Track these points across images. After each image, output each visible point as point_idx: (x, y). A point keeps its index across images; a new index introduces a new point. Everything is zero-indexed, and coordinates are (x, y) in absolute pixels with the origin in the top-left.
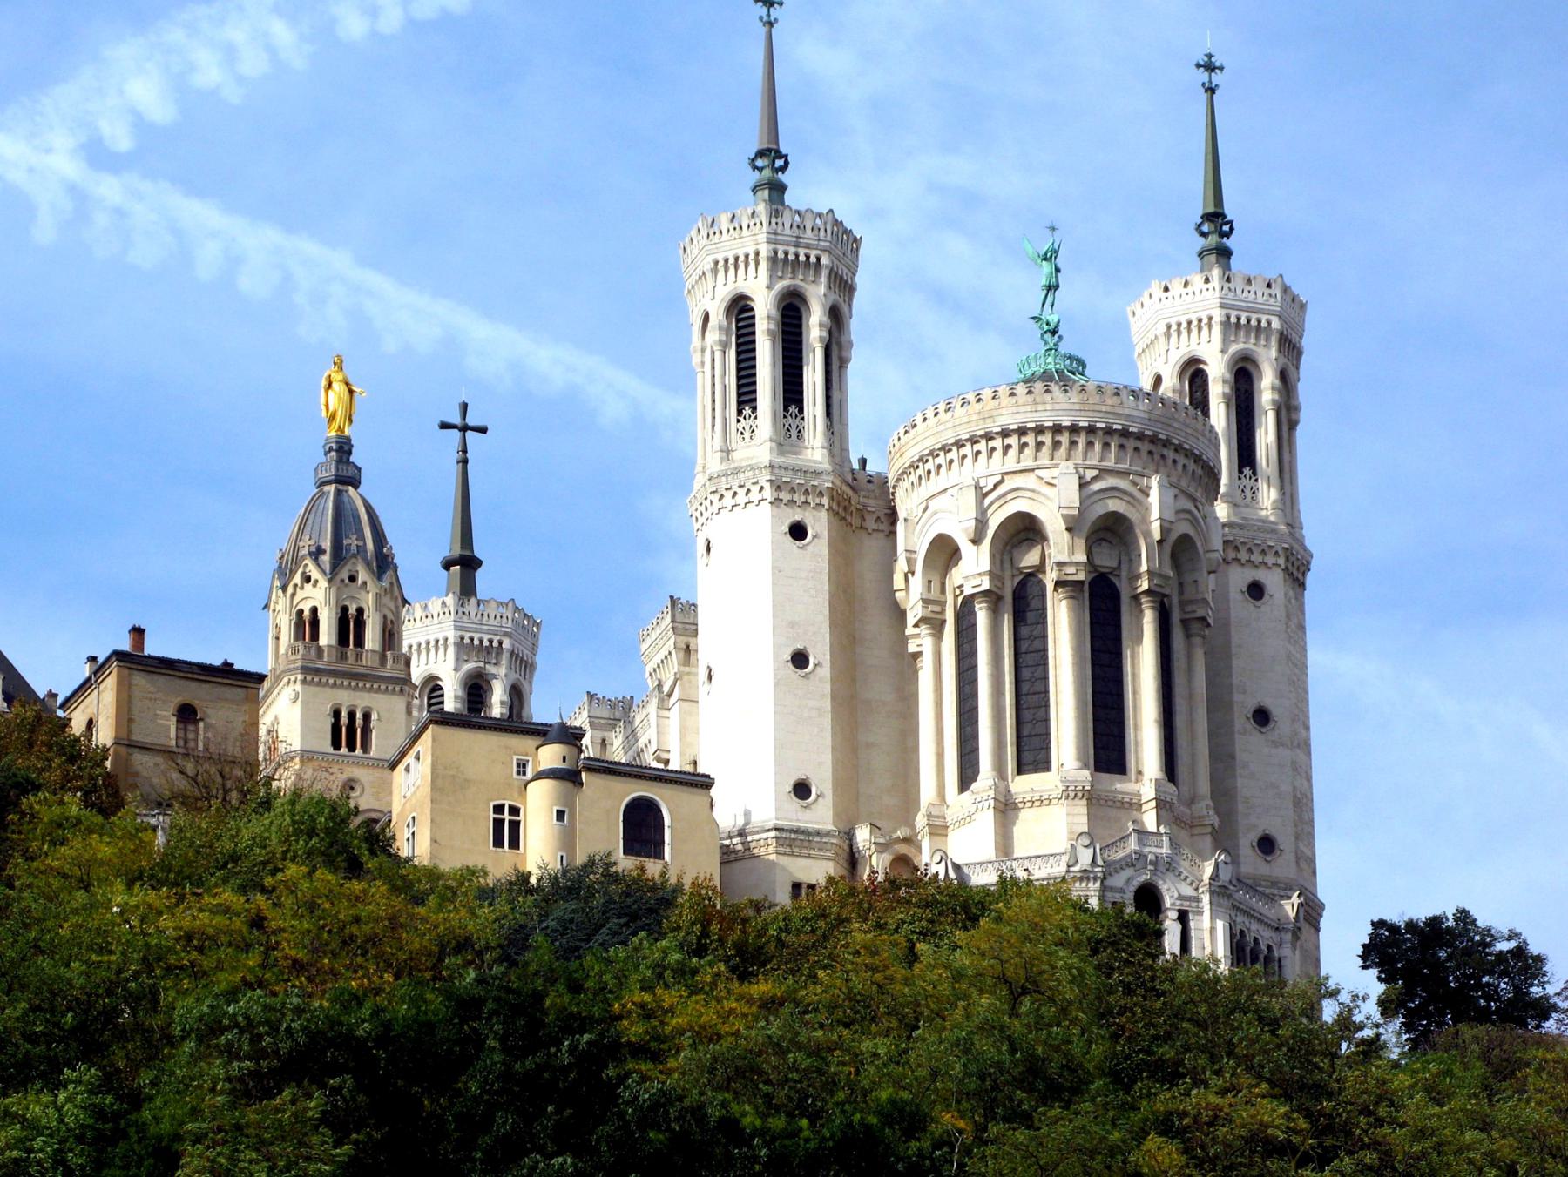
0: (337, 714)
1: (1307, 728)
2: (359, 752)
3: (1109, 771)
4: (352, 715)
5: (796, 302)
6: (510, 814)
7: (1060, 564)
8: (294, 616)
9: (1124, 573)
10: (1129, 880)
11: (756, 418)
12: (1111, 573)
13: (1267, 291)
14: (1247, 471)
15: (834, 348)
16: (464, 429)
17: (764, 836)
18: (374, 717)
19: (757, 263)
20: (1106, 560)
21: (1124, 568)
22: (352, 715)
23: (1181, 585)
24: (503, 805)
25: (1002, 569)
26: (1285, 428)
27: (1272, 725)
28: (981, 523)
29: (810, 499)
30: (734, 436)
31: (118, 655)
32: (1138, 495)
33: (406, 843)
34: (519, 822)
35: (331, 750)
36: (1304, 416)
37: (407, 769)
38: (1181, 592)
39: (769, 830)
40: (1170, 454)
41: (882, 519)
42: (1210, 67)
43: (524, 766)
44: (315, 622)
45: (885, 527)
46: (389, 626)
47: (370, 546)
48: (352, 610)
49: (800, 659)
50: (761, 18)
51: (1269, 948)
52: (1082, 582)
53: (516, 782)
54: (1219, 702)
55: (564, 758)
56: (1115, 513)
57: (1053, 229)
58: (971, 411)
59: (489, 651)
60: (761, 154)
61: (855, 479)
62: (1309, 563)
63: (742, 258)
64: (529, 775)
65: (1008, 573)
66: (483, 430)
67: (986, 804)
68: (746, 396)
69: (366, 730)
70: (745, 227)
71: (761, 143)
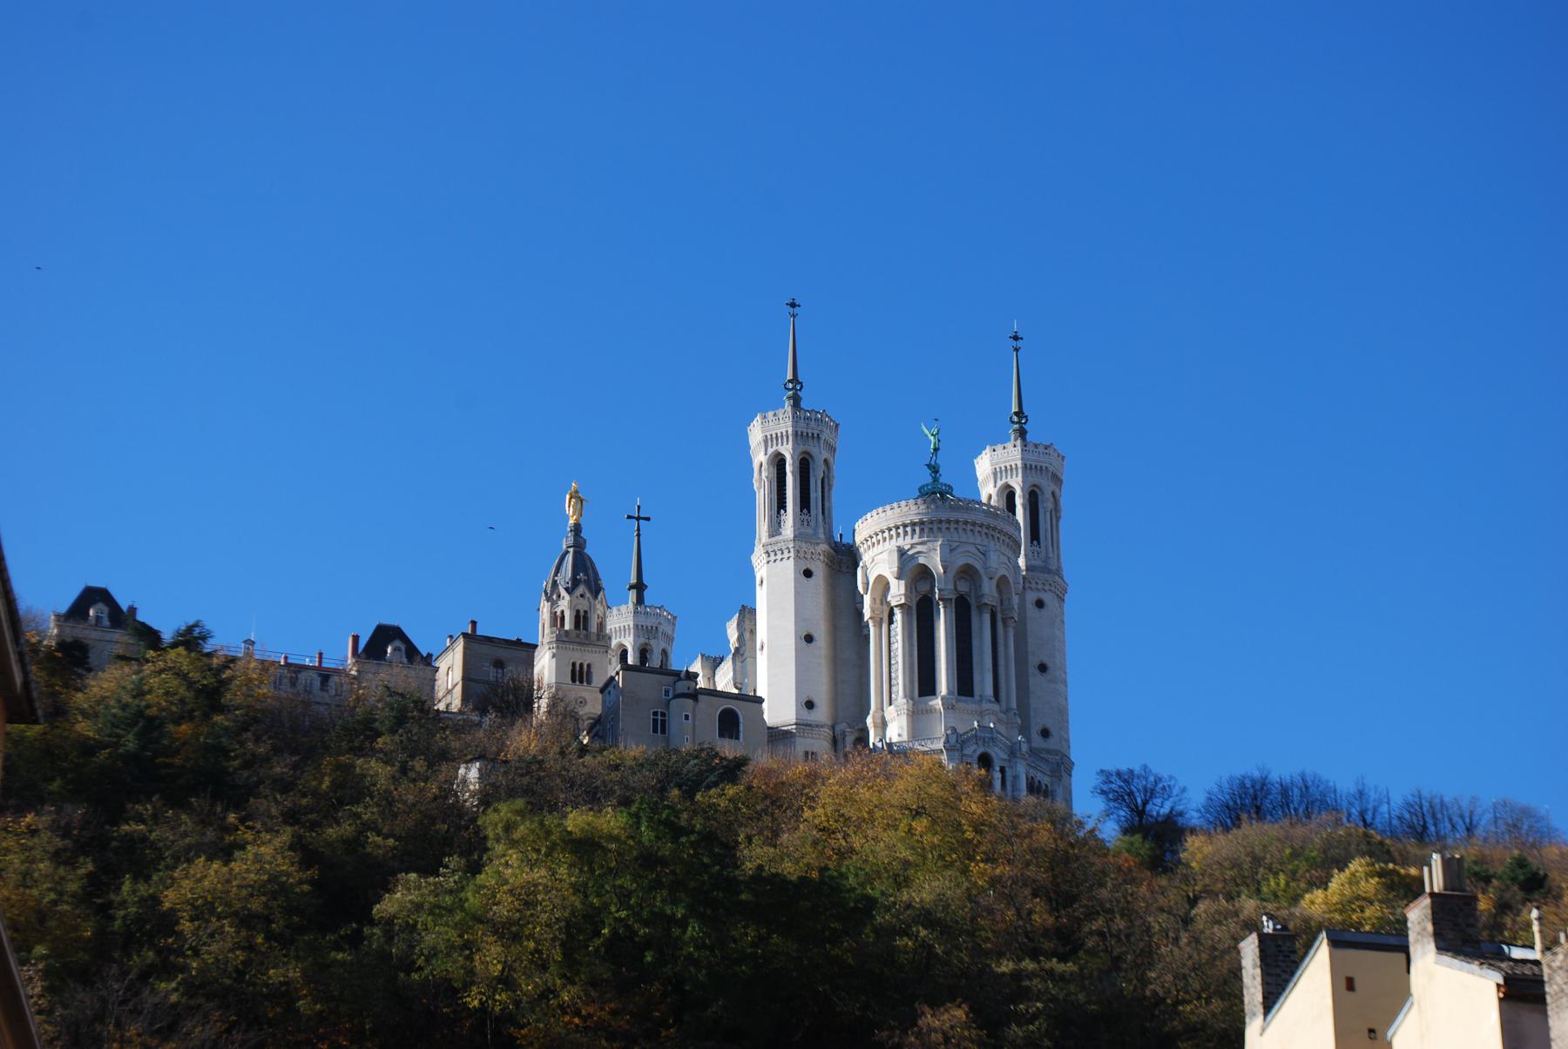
0: (574, 664)
2: (585, 684)
3: (965, 695)
4: (581, 665)
5: (807, 456)
9: (973, 595)
14: (1035, 542)
15: (826, 480)
16: (638, 519)
20: (963, 587)
21: (973, 592)
22: (581, 665)
23: (1001, 601)
25: (911, 592)
27: (1048, 672)
31: (465, 635)
32: (982, 557)
37: (609, 692)
38: (1002, 604)
44: (563, 618)
48: (582, 613)
49: (809, 639)
52: (951, 599)
54: (1021, 660)
56: (968, 564)
64: (671, 696)
68: (781, 504)
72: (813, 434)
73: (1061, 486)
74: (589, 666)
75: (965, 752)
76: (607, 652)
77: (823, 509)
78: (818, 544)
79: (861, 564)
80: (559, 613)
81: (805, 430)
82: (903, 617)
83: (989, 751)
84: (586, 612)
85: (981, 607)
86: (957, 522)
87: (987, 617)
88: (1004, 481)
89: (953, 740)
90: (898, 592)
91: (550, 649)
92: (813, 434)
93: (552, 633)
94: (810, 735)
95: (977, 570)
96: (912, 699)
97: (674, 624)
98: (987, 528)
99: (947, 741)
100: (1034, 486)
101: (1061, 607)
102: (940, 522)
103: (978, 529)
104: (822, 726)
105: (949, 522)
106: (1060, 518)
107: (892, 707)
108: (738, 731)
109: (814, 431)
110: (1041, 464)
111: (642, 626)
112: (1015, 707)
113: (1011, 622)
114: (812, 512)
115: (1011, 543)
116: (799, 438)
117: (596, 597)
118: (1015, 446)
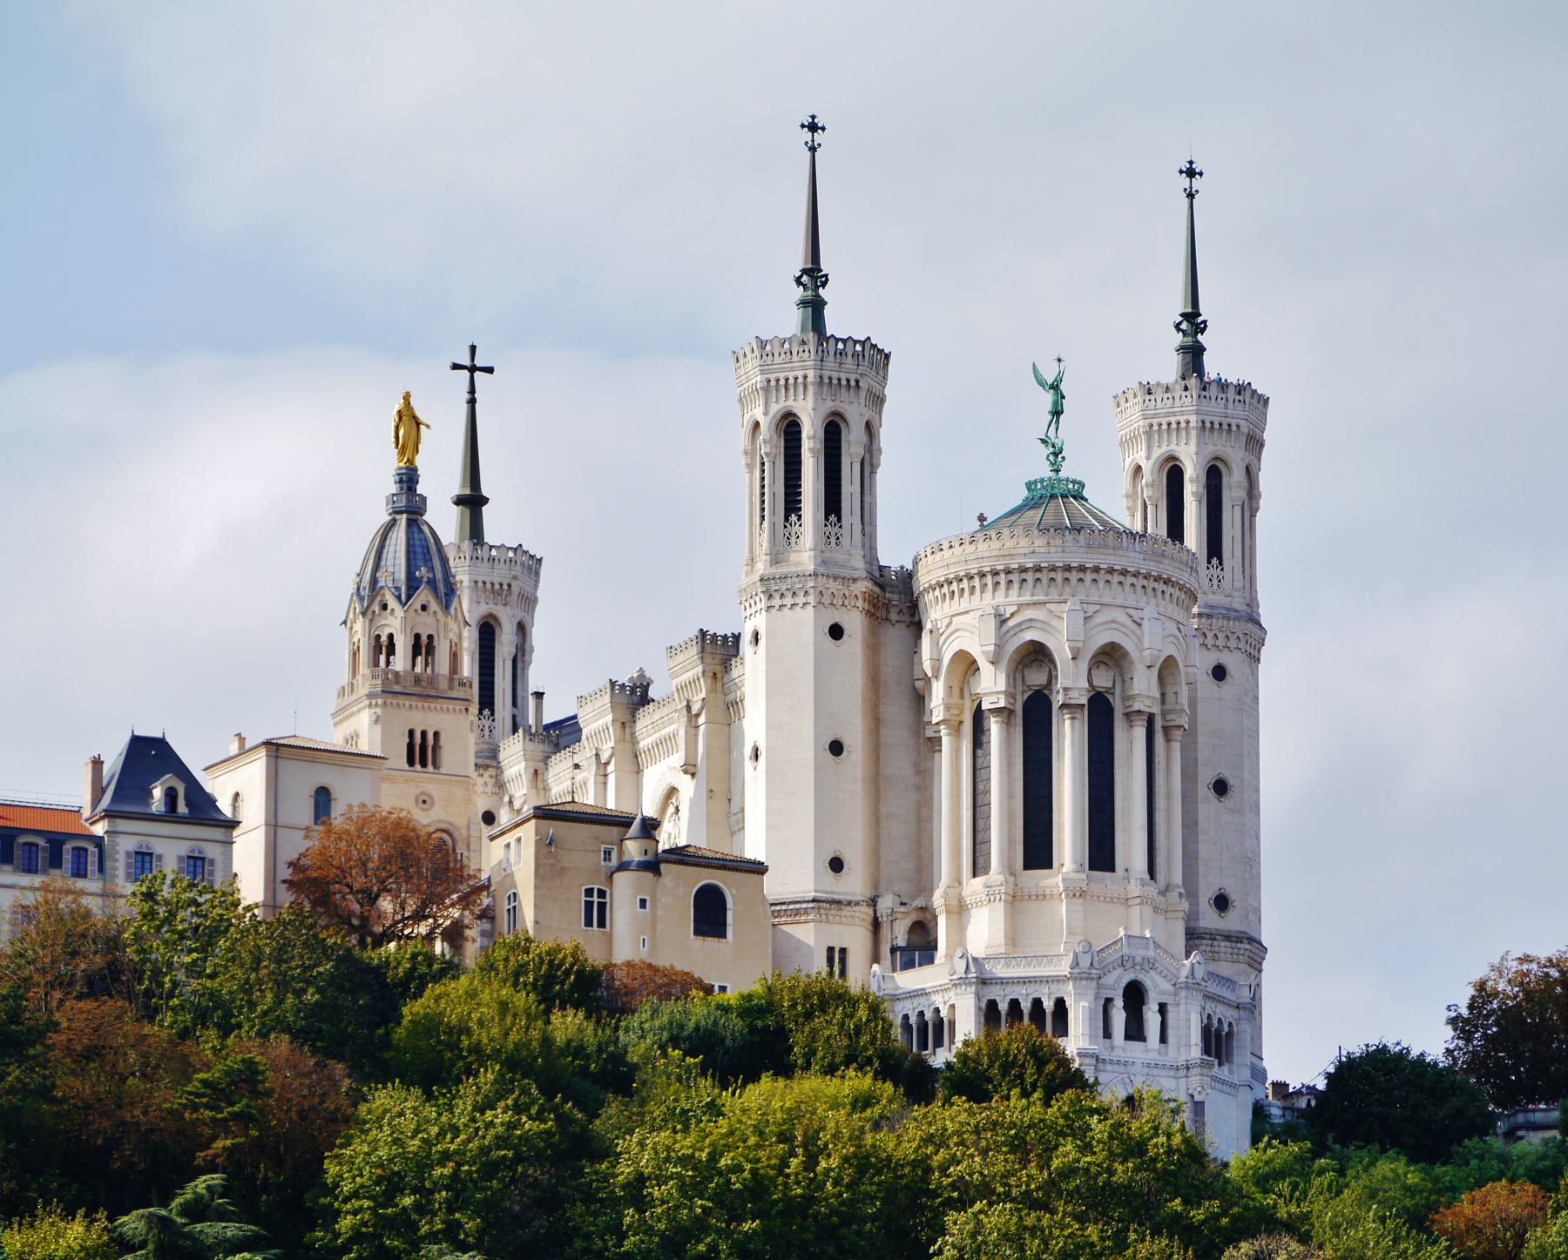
0: (411, 733)
1: (1257, 790)
2: (430, 768)
4: (424, 734)
5: (837, 419)
6: (598, 897)
7: (1065, 689)
8: (373, 640)
9: (1118, 692)
10: (1120, 978)
11: (800, 525)
12: (1107, 692)
13: (1238, 397)
14: (1215, 561)
16: (473, 369)
17: (804, 906)
18: (442, 737)
19: (805, 387)
20: (1103, 680)
22: (424, 734)
24: (593, 889)
25: (1015, 687)
26: (1247, 516)
27: (1230, 793)
28: (999, 647)
29: (846, 603)
30: (784, 542)
32: (1133, 626)
33: (506, 913)
34: (605, 903)
35: (406, 767)
36: (1263, 503)
39: (808, 902)
40: (1160, 587)
41: (904, 611)
42: (1191, 173)
43: (610, 853)
44: (391, 649)
45: (906, 618)
46: (454, 649)
47: (439, 576)
48: (424, 639)
49: (836, 748)
50: (806, 143)
51: (1230, 1024)
52: (1083, 705)
53: (604, 870)
55: (646, 851)
57: (1059, 360)
58: (992, 547)
59: (499, 592)
60: (804, 271)
61: (882, 576)
62: (1264, 640)
63: (791, 381)
64: (614, 861)
65: (1020, 689)
66: (490, 370)
67: (998, 897)
68: (792, 504)
69: (436, 747)
70: (795, 353)
71: (805, 263)
72: (848, 380)
73: (1260, 452)
74: (436, 734)
75: (1102, 981)
76: (467, 710)
77: (862, 509)
78: (855, 580)
79: (928, 626)
80: (384, 638)
81: (835, 375)
82: (1001, 731)
83: (1142, 977)
84: (430, 637)
85: (1129, 716)
86: (1097, 569)
87: (1140, 732)
88: (1164, 449)
89: (1085, 962)
90: (992, 685)
91: (370, 706)
92: (848, 380)
93: (374, 677)
94: (838, 918)
95: (1127, 652)
96: (1012, 874)
97: (537, 574)
98: (1145, 578)
99: (1076, 964)
100: (1217, 458)
101: (1255, 675)
102: (1068, 568)
103: (1130, 580)
104: (857, 904)
105: (1082, 569)
106: (1258, 509)
107: (980, 880)
108: (724, 924)
109: (849, 376)
110: (1228, 420)
111: (484, 583)
112: (1181, 883)
113: (1178, 734)
114: (843, 518)
115: (1183, 596)
116: (825, 388)
117: (446, 607)
118: (1186, 389)
